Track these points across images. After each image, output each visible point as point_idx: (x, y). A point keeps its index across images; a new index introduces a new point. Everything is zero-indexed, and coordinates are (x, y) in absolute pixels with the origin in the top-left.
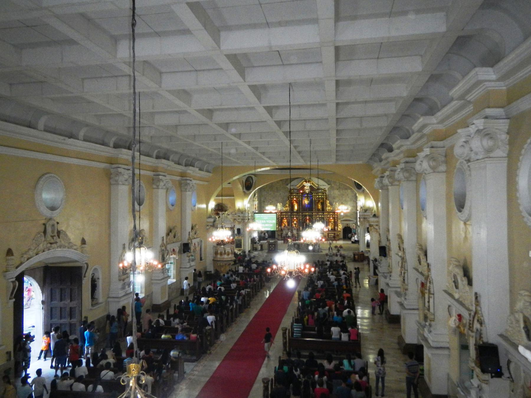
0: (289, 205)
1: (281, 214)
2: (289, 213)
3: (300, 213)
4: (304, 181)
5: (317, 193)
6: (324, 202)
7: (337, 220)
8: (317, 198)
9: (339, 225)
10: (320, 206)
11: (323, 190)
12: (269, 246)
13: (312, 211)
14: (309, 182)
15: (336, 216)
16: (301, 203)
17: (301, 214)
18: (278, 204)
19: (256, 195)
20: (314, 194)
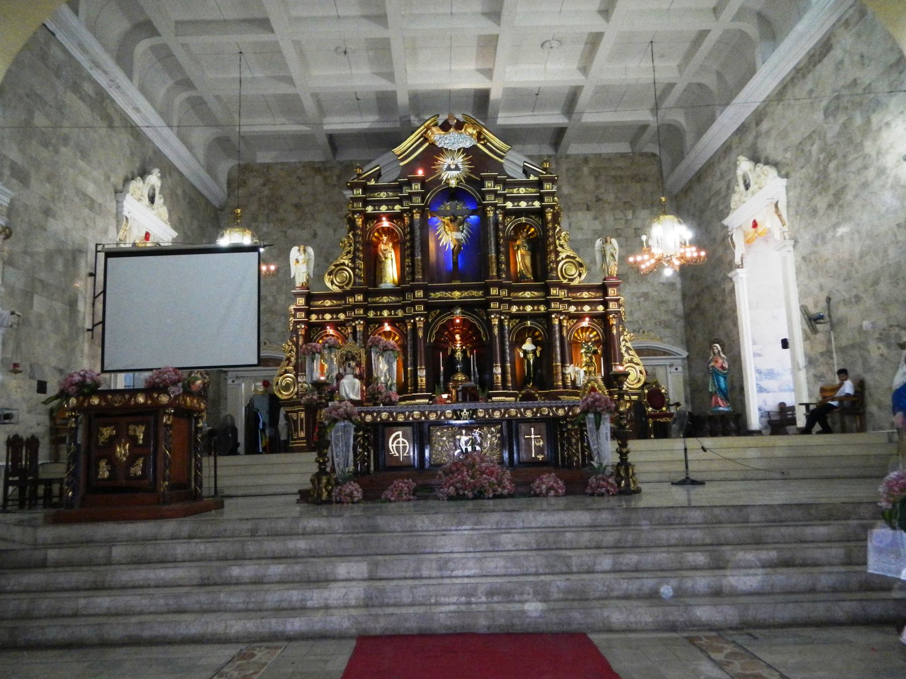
0: (353, 260)
1: (307, 303)
2: (352, 293)
3: (412, 290)
4: (436, 125)
5: (506, 185)
6: (545, 237)
7: (620, 334)
8: (507, 213)
9: (627, 357)
10: (522, 259)
11: (536, 173)
12: (91, 434)
13: (487, 276)
14: (459, 126)
15: (613, 306)
16: (418, 232)
17: (420, 294)
18: (295, 253)
19: (154, 179)
20: (489, 185)
